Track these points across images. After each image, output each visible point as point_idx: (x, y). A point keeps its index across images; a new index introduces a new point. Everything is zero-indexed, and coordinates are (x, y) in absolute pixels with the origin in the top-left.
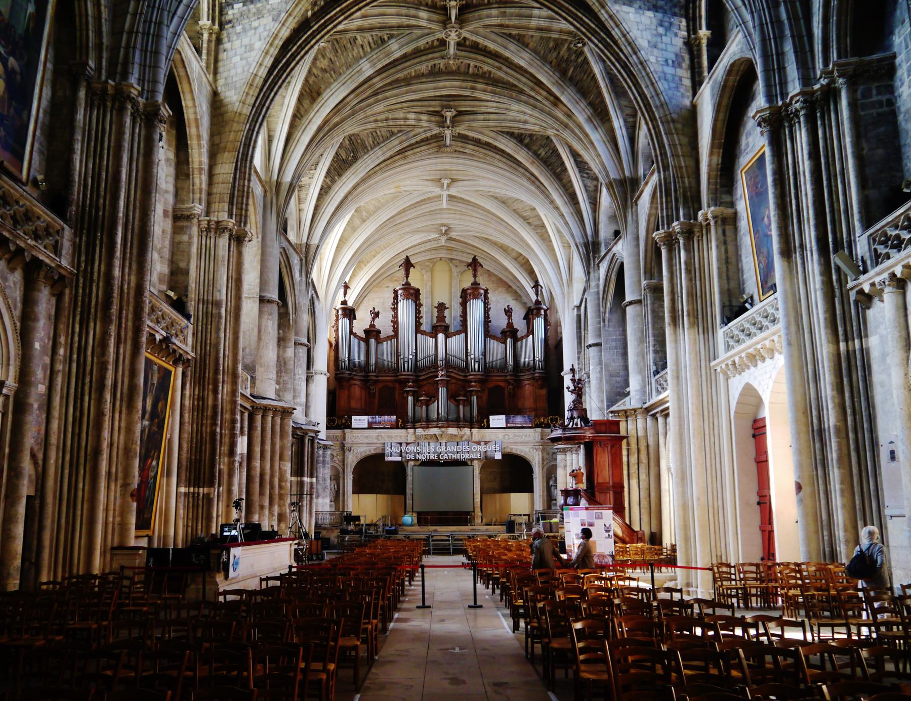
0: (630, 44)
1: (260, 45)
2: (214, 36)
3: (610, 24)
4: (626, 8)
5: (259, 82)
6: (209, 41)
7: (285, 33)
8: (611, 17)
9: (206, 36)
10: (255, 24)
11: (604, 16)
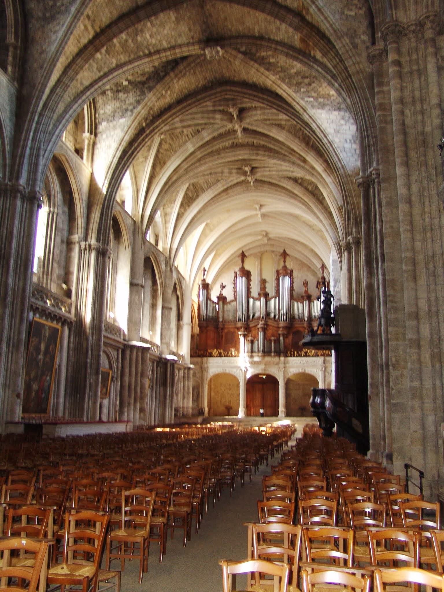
0: (322, 132)
1: (114, 145)
2: (91, 142)
3: (310, 121)
4: (320, 111)
5: (113, 166)
6: (89, 144)
7: (127, 138)
8: (310, 117)
9: (86, 142)
10: (112, 133)
11: (306, 117)
